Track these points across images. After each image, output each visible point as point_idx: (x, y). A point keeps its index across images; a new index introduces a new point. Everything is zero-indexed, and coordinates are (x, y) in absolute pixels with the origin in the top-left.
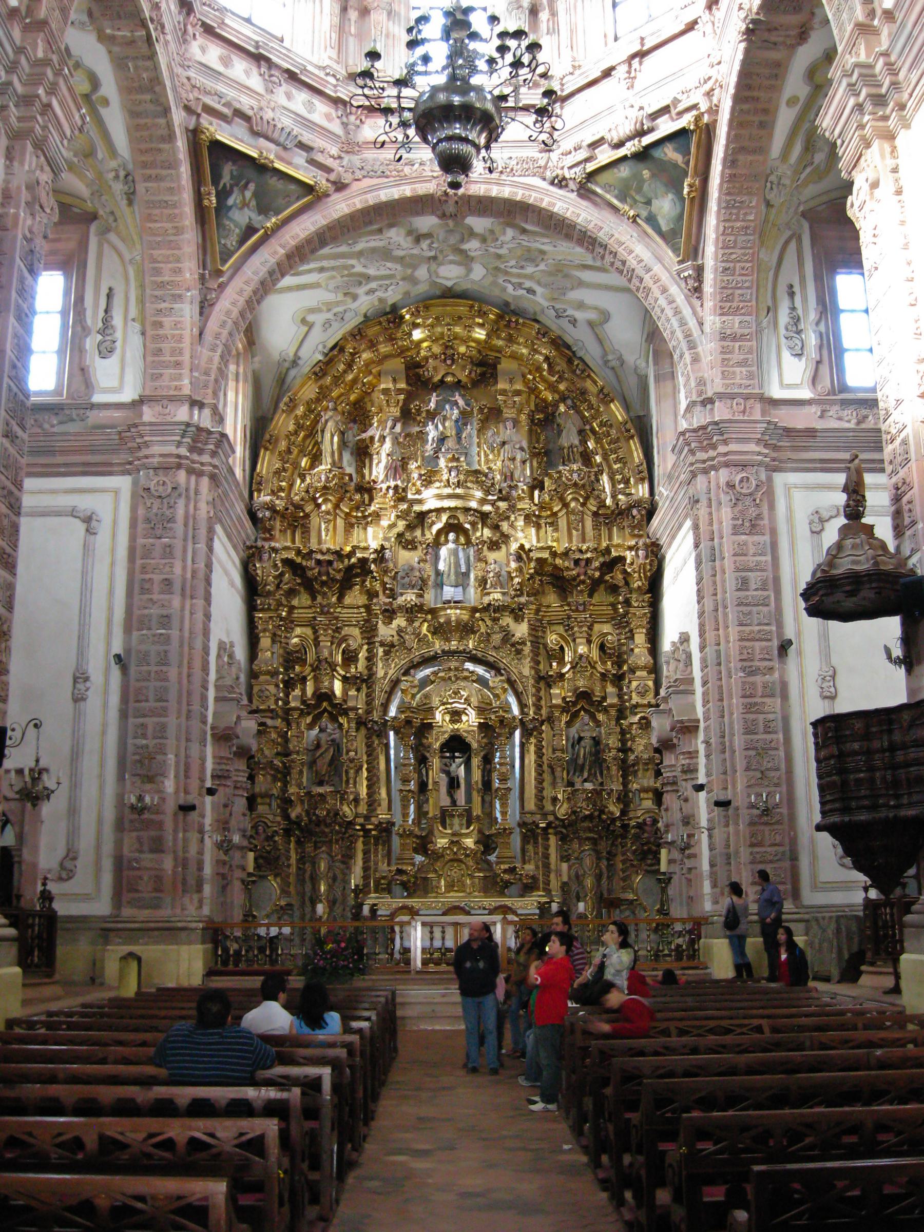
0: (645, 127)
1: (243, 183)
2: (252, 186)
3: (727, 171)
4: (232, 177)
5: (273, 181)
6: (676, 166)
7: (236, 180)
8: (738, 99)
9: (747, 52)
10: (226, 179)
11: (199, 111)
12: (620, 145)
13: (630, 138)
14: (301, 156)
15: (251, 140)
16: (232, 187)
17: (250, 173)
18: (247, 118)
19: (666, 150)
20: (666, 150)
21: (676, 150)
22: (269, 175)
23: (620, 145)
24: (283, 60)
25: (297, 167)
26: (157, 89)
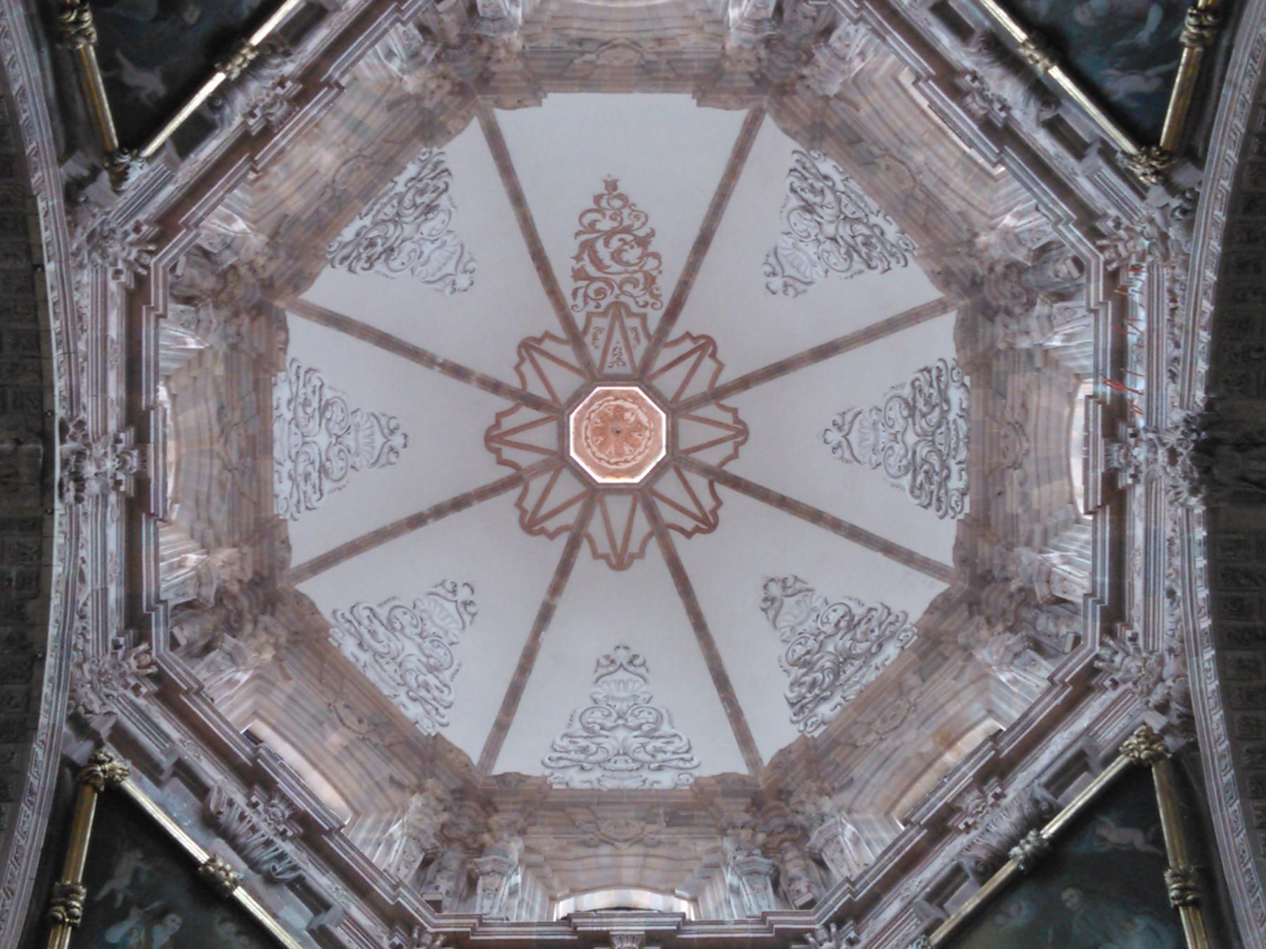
0: (1044, 806)
1: (156, 905)
2: (173, 922)
3: (1253, 804)
4: (134, 884)
5: (226, 930)
6: (1133, 853)
7: (141, 895)
8: (1225, 638)
9: (1212, 518)
10: (120, 883)
11: (105, 732)
12: (999, 858)
13: (1014, 842)
14: (300, 911)
15: (197, 832)
16: (127, 904)
17: (176, 890)
18: (200, 789)
19: (1103, 831)
20: (1103, 831)
21: (1125, 823)
22: (218, 915)
23: (999, 858)
24: (299, 794)
25: (286, 926)
26: (31, 607)
